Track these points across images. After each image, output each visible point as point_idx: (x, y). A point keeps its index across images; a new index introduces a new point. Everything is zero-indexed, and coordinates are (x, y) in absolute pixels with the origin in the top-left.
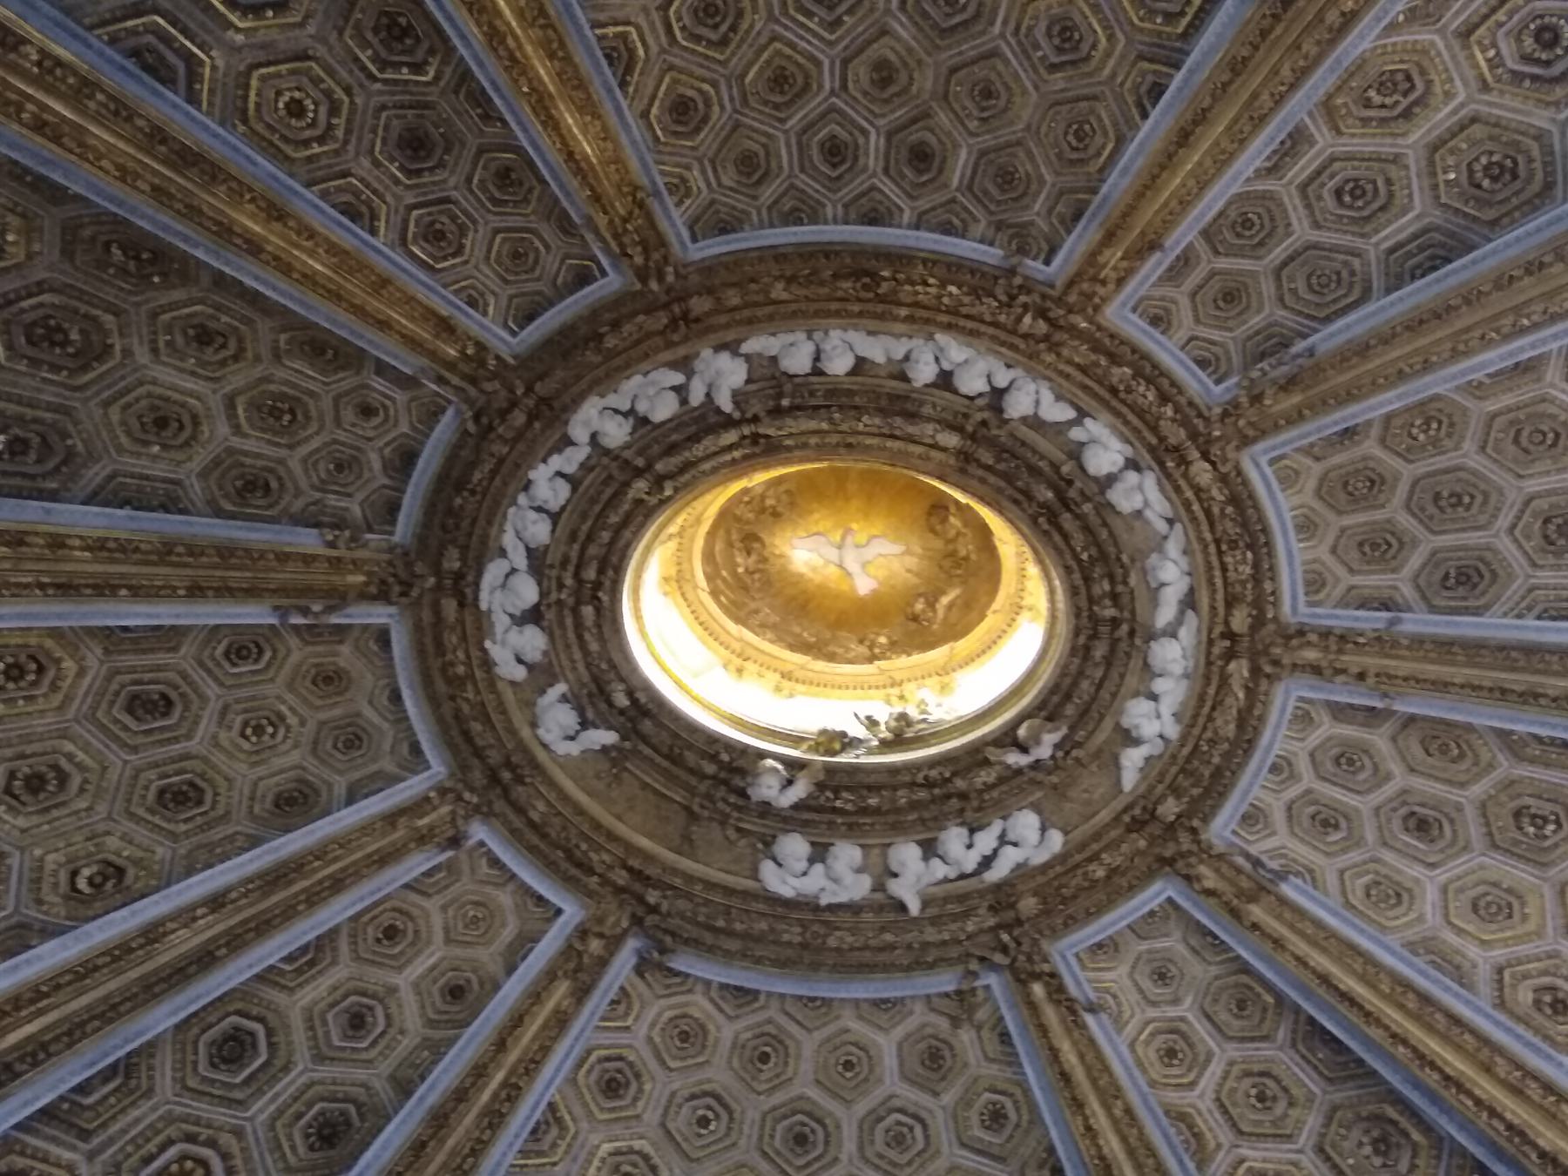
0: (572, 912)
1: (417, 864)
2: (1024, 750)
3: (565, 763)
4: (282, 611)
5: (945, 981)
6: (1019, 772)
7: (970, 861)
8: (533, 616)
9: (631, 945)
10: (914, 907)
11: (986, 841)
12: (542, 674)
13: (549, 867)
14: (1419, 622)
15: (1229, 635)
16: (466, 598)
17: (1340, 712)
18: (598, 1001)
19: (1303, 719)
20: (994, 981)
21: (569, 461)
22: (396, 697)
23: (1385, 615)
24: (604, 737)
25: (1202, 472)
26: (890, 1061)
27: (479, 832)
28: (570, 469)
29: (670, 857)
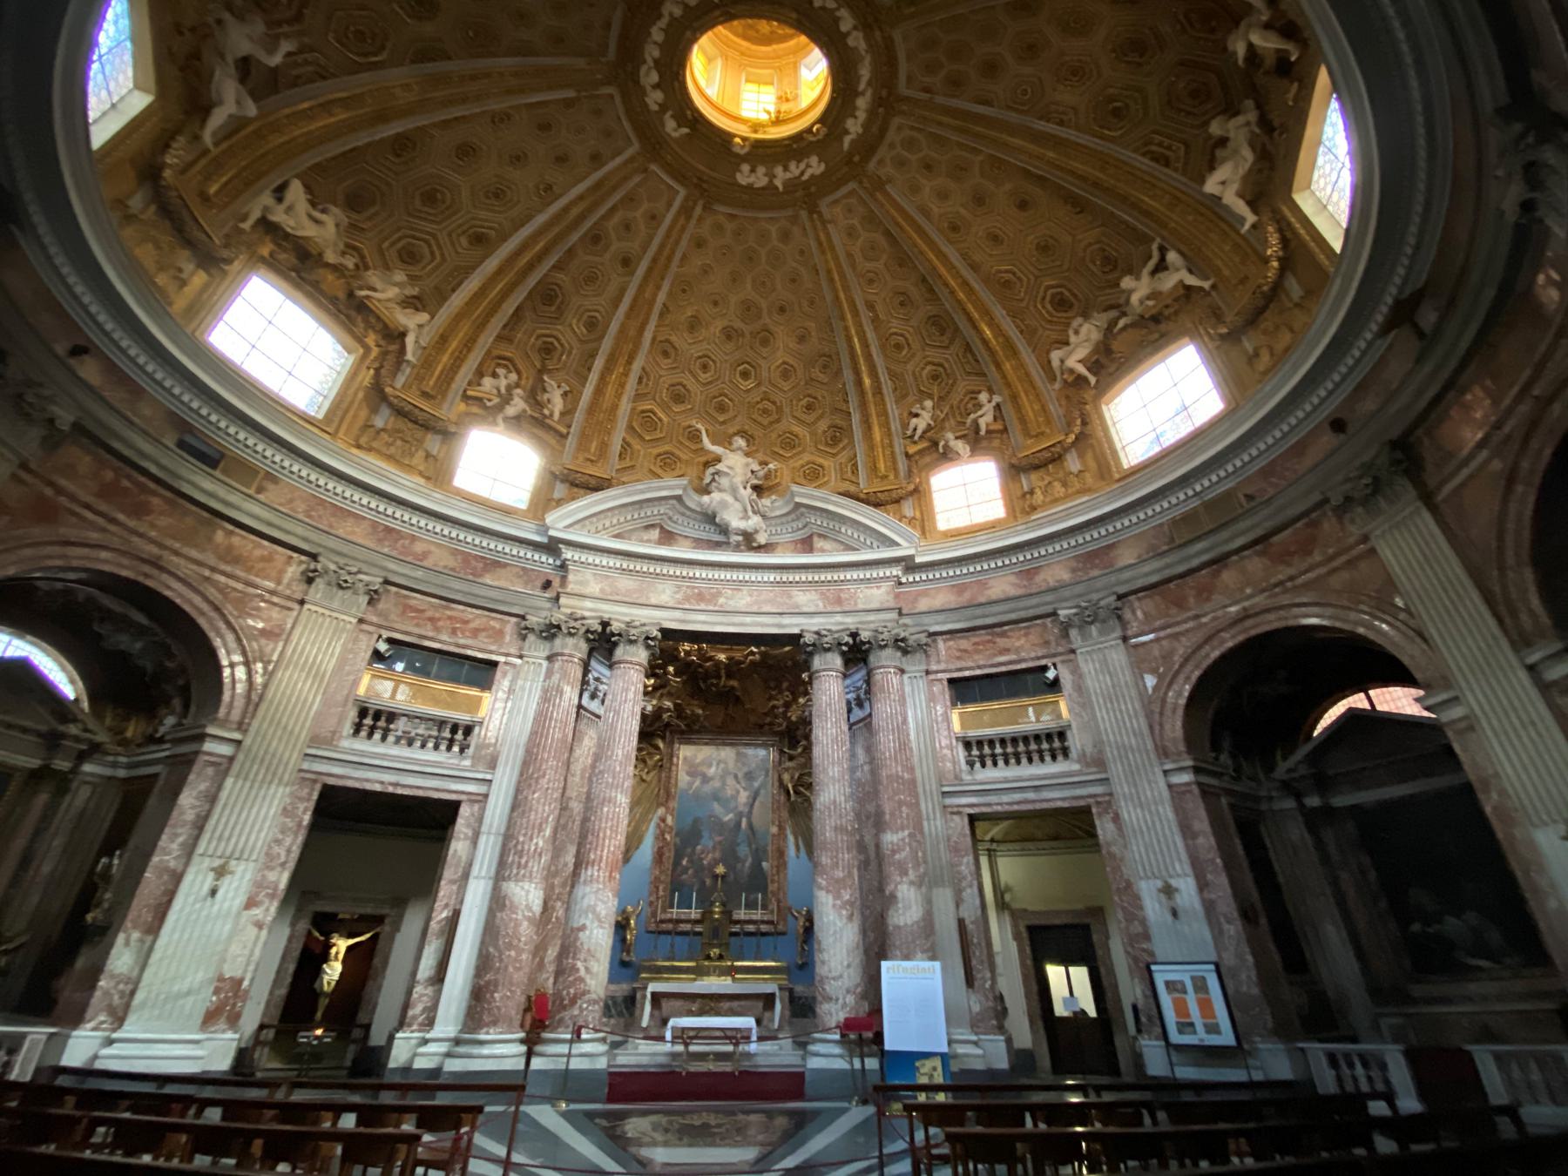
0: (682, 192)
1: (637, 179)
2: (814, 135)
3: (676, 140)
4: (579, 91)
5: (789, 212)
6: (811, 142)
7: (797, 173)
8: (656, 86)
9: (700, 203)
10: (781, 188)
11: (802, 166)
12: (663, 108)
13: (675, 178)
14: (940, 99)
15: (880, 98)
16: (637, 82)
17: (912, 128)
18: (693, 221)
19: (899, 128)
20: (804, 214)
21: (663, 23)
22: (619, 118)
23: (928, 95)
24: (685, 130)
25: (878, 34)
26: (774, 235)
27: (653, 167)
28: (664, 26)
29: (707, 171)
